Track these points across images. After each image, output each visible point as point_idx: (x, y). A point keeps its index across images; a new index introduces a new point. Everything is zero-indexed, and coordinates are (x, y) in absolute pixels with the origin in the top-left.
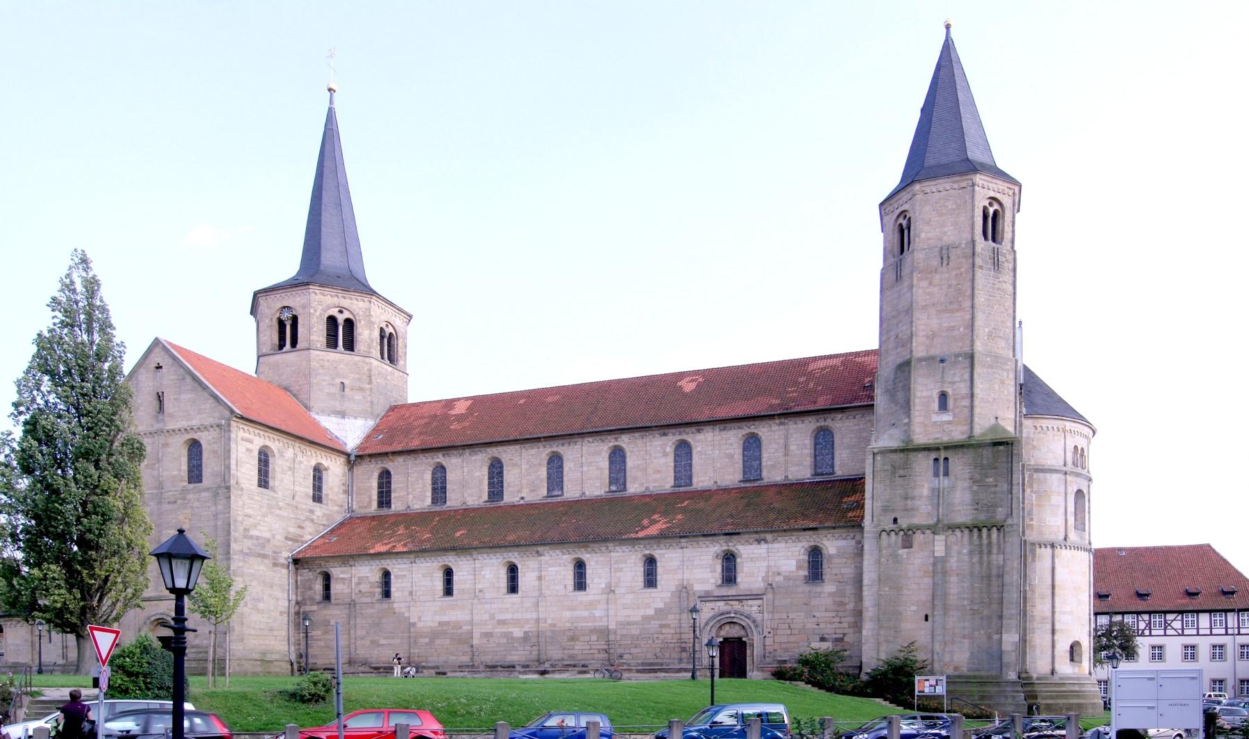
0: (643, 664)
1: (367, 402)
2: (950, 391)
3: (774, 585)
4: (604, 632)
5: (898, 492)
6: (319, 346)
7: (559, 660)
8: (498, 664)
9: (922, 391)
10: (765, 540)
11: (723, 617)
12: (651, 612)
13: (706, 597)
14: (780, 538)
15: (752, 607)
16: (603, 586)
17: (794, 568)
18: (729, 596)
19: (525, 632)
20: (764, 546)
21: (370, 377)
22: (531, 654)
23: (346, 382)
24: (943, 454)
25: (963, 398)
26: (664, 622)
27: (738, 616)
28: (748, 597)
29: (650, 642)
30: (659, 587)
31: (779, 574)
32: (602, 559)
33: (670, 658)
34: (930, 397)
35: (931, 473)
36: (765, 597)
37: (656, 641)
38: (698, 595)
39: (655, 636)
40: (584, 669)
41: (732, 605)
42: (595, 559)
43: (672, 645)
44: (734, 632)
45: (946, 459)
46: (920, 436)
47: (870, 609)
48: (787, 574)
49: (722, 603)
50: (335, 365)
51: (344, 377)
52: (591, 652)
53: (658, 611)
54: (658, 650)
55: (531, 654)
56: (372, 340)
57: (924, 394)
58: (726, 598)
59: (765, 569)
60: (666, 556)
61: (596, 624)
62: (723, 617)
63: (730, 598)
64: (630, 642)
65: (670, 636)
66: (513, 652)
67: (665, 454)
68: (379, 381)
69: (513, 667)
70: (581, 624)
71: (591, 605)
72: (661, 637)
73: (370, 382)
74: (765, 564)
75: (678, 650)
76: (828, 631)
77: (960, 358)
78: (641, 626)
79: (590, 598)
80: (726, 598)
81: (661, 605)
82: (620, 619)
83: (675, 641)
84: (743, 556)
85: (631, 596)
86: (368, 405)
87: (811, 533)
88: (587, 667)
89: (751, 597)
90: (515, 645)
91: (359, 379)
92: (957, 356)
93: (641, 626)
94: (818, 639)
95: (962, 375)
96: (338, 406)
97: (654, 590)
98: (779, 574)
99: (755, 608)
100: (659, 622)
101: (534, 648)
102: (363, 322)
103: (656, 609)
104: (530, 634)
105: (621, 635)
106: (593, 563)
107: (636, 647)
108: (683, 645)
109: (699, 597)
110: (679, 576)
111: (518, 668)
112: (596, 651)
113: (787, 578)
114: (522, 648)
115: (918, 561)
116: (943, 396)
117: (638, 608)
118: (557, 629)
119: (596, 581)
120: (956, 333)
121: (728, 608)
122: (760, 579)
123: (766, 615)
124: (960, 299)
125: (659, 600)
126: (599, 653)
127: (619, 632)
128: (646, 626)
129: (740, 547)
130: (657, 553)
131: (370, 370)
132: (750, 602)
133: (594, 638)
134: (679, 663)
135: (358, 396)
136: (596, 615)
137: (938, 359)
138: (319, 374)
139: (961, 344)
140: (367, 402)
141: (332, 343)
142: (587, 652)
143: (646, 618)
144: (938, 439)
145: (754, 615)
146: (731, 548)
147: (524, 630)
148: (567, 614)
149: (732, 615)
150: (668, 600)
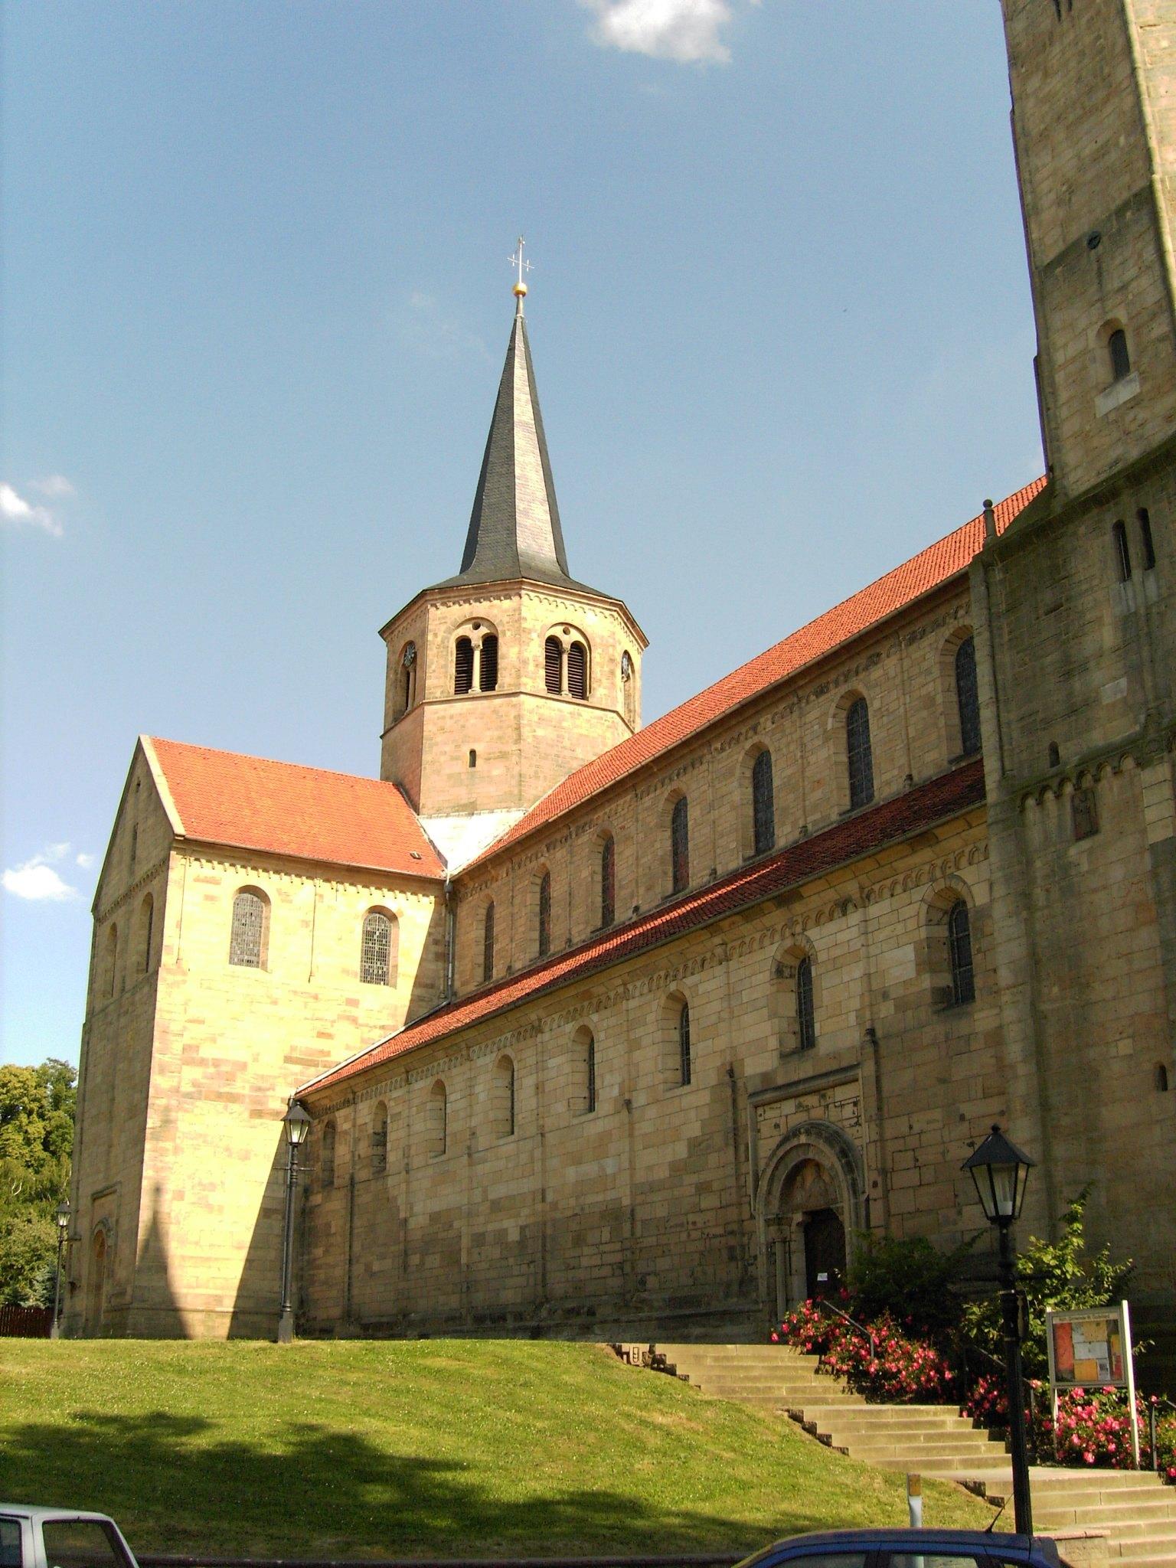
1: (512, 777)
2: (1121, 315)
3: (879, 1033)
4: (614, 1215)
5: (1049, 659)
6: (438, 694)
9: (1065, 345)
11: (787, 1146)
17: (910, 972)
21: (518, 728)
23: (479, 749)
24: (1126, 508)
25: (1154, 316)
34: (1085, 351)
35: (1112, 572)
36: (859, 1072)
45: (1143, 515)
46: (1080, 472)
47: (1022, 1070)
49: (789, 1107)
50: (461, 723)
51: (477, 740)
53: (694, 1144)
56: (525, 662)
57: (1071, 351)
58: (793, 1090)
62: (787, 1146)
63: (801, 1088)
67: (827, 737)
68: (540, 732)
70: (591, 1199)
73: (519, 738)
74: (857, 971)
77: (1129, 214)
82: (641, 1176)
86: (514, 782)
91: (500, 738)
92: (1120, 212)
95: (1140, 256)
96: (463, 795)
98: (885, 996)
99: (848, 1111)
100: (694, 1179)
102: (508, 634)
110: (721, 1043)
113: (901, 1006)
115: (1117, 873)
116: (1116, 338)
118: (558, 1215)
120: (1113, 156)
122: (852, 1018)
124: (1106, 70)
127: (640, 1214)
131: (518, 717)
135: (497, 771)
137: (1085, 243)
138: (437, 744)
139: (1126, 178)
140: (512, 777)
141: (463, 683)
143: (678, 1168)
144: (1116, 462)
147: (522, 1222)
148: (571, 1173)
149: (803, 1139)
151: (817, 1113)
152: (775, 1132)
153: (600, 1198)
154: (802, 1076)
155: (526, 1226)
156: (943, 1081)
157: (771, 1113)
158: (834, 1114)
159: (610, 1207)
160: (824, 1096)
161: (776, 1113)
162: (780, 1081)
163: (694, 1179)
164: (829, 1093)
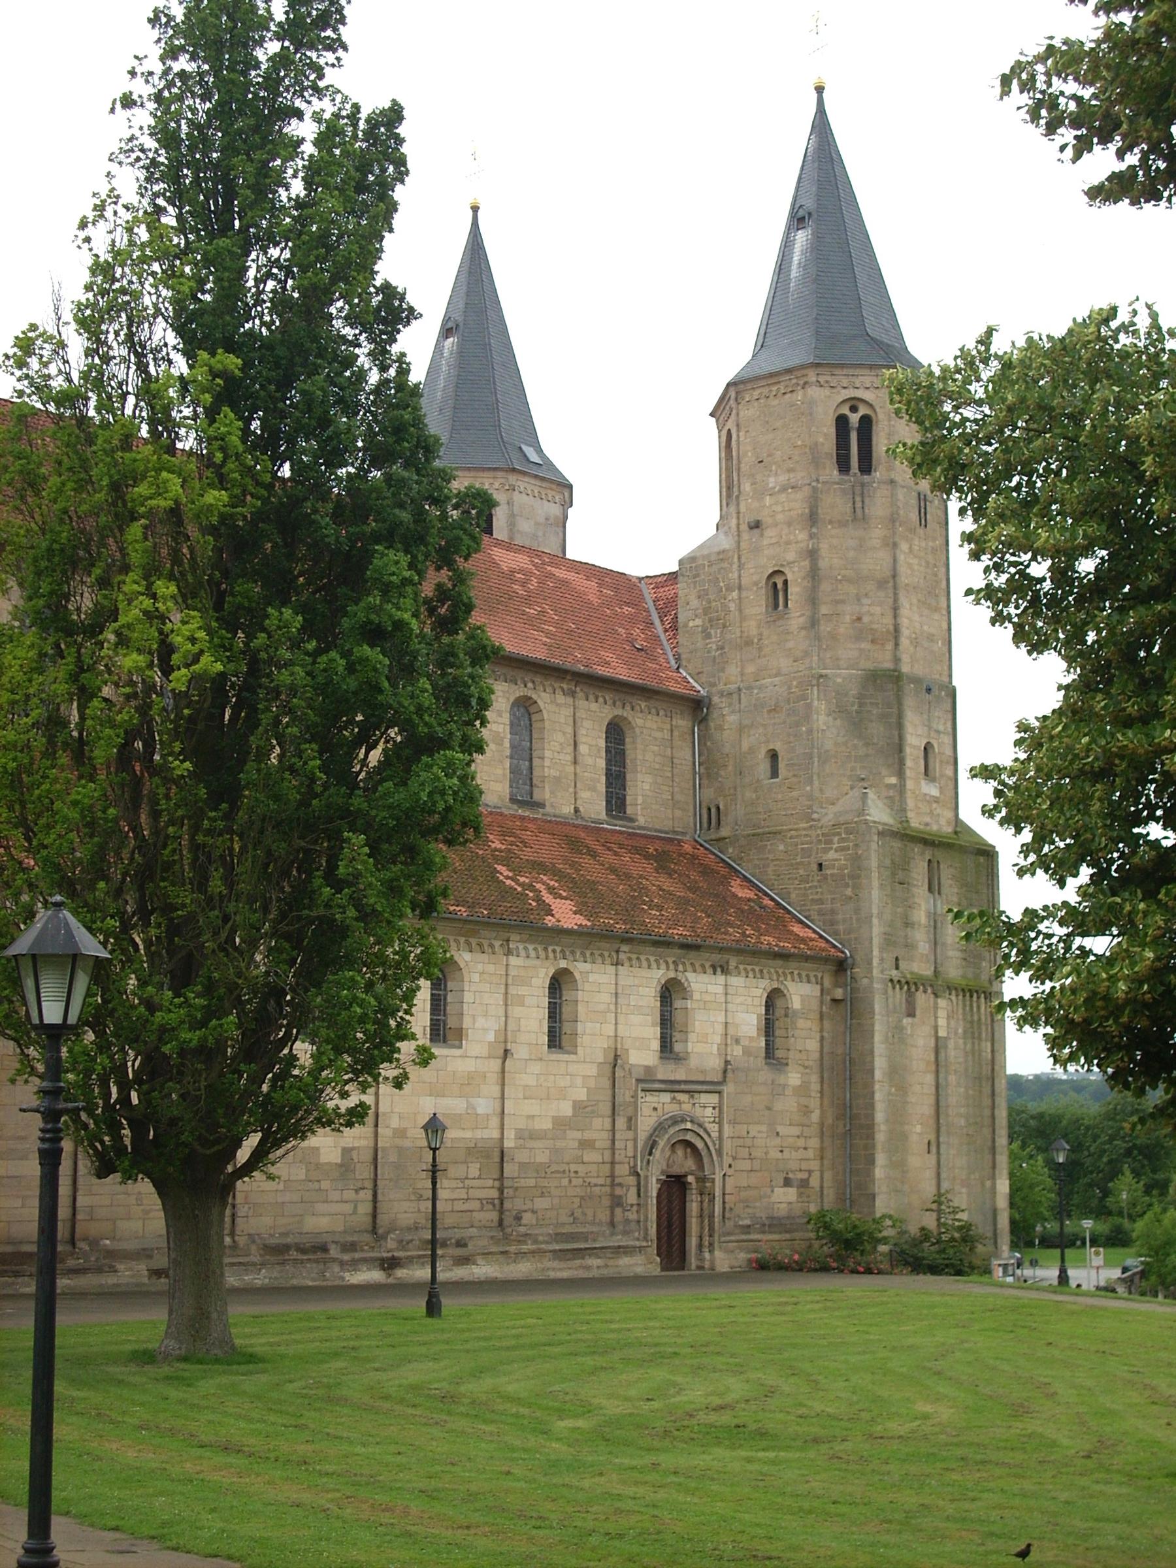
0: (559, 1237)
7: (409, 1229)
8: (289, 1240)
10: (725, 971)
12: (566, 1109)
13: (648, 1082)
14: (741, 967)
15: (705, 1108)
16: (491, 1037)
18: (679, 1082)
19: (346, 1151)
20: (721, 979)
22: (355, 1212)
26: (587, 1135)
27: (696, 1128)
28: (705, 1088)
29: (565, 1182)
30: (580, 1050)
31: (737, 1041)
32: (491, 968)
33: (593, 1223)
37: (575, 1182)
38: (635, 1075)
39: (573, 1167)
40: (459, 1252)
41: (680, 1103)
42: (480, 967)
43: (597, 1190)
44: (684, 1164)
48: (747, 1043)
49: (666, 1097)
52: (467, 1206)
53: (578, 1106)
54: (577, 1200)
55: (355, 1212)
58: (677, 1087)
59: (720, 1029)
60: (592, 978)
61: (479, 1134)
63: (683, 1087)
64: (532, 1182)
65: (594, 1168)
66: (321, 1207)
69: (324, 1249)
71: (469, 1084)
72: (581, 1169)
75: (606, 1202)
76: (793, 1165)
78: (549, 1143)
79: (469, 1066)
80: (677, 1087)
81: (581, 1095)
83: (601, 1181)
84: (696, 996)
85: (536, 1068)
87: (780, 962)
88: (465, 1245)
89: (705, 1088)
90: (325, 1185)
93: (549, 1143)
94: (782, 1182)
97: (573, 1057)
98: (737, 1041)
99: (709, 1111)
100: (578, 1135)
101: (362, 1193)
103: (574, 1102)
104: (354, 1155)
105: (522, 1165)
106: (476, 977)
107: (542, 1195)
108: (618, 1191)
109: (639, 1081)
111: (334, 1252)
112: (476, 1205)
113: (747, 1052)
114: (335, 1195)
117: (548, 1099)
118: (407, 1143)
119: (481, 1022)
121: (673, 1109)
122: (715, 1047)
123: (726, 1126)
125: (579, 1081)
126: (482, 1209)
128: (560, 1144)
129: (691, 976)
130: (579, 968)
132: (704, 1098)
133: (474, 1170)
134: (612, 1234)
136: (480, 1111)
142: (460, 1206)
143: (561, 1124)
145: (709, 1126)
146: (680, 976)
150: (592, 1084)
151: (687, 1107)
152: (654, 1114)
153: (468, 1134)
154: (678, 1078)
155: (353, 1149)
156: (769, 1109)
157: (651, 1099)
158: (698, 1112)
159: (479, 1145)
160: (692, 1097)
161: (655, 1099)
162: (660, 1077)
163: (578, 1135)
164: (696, 1095)
